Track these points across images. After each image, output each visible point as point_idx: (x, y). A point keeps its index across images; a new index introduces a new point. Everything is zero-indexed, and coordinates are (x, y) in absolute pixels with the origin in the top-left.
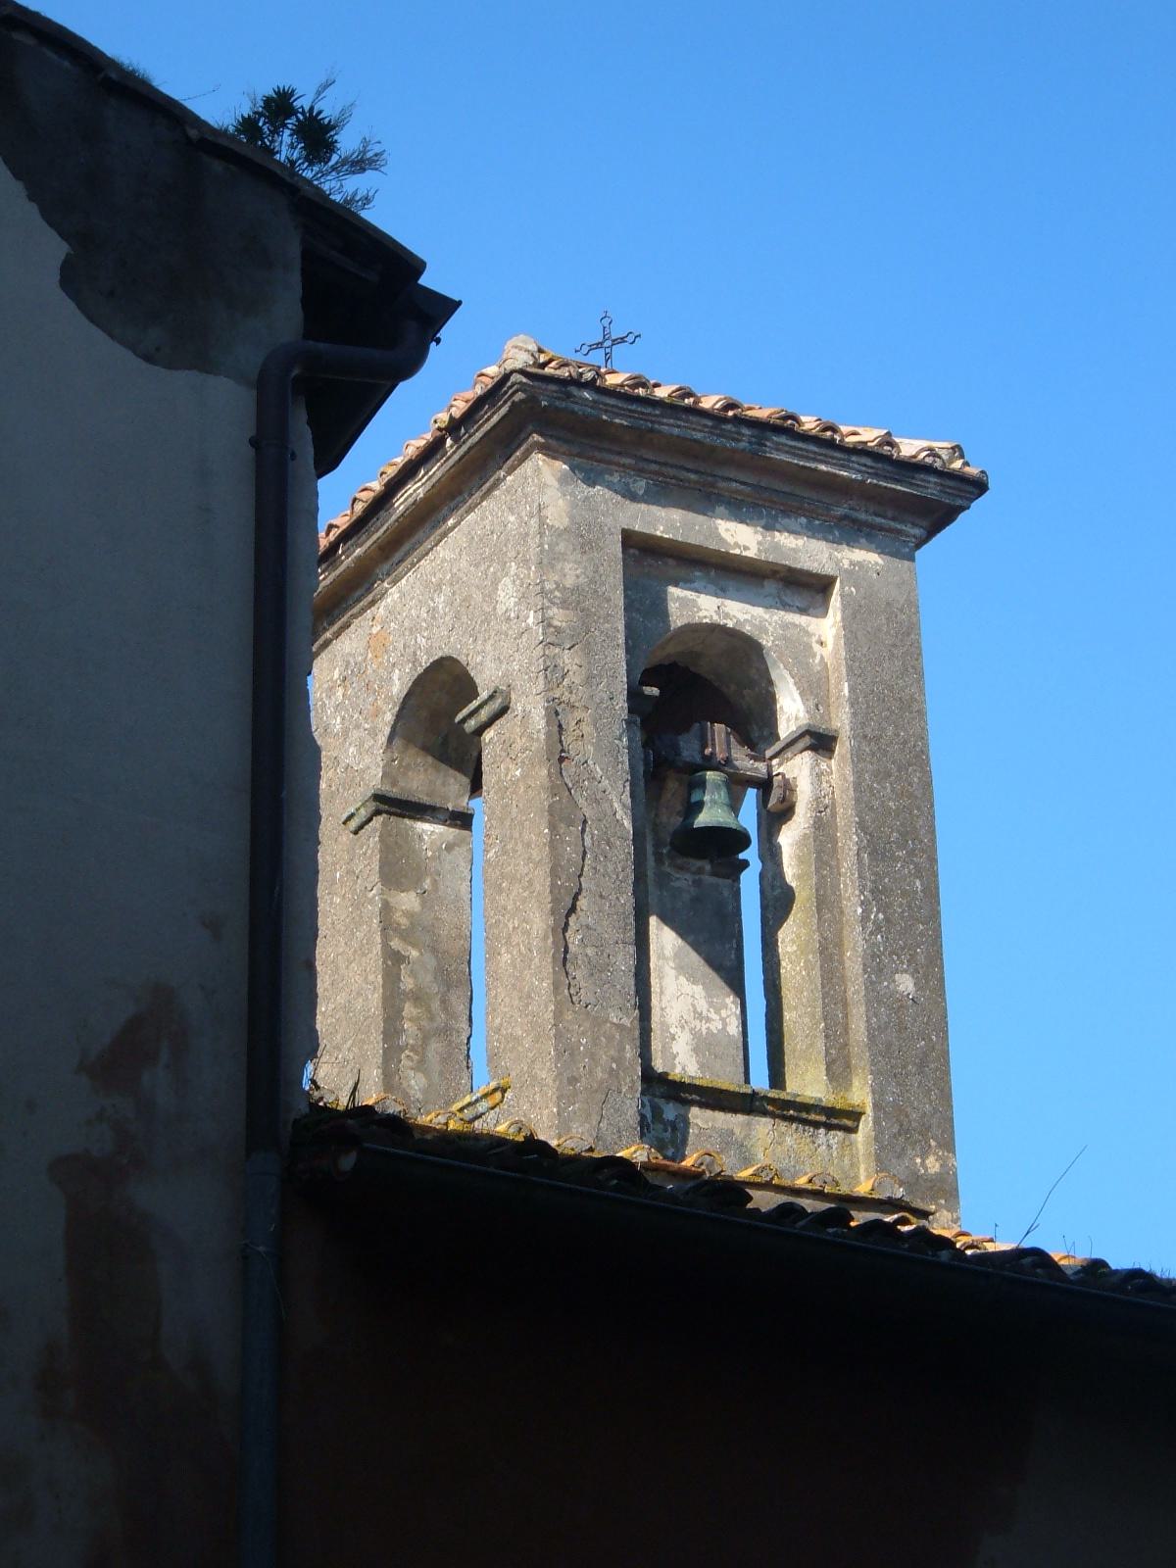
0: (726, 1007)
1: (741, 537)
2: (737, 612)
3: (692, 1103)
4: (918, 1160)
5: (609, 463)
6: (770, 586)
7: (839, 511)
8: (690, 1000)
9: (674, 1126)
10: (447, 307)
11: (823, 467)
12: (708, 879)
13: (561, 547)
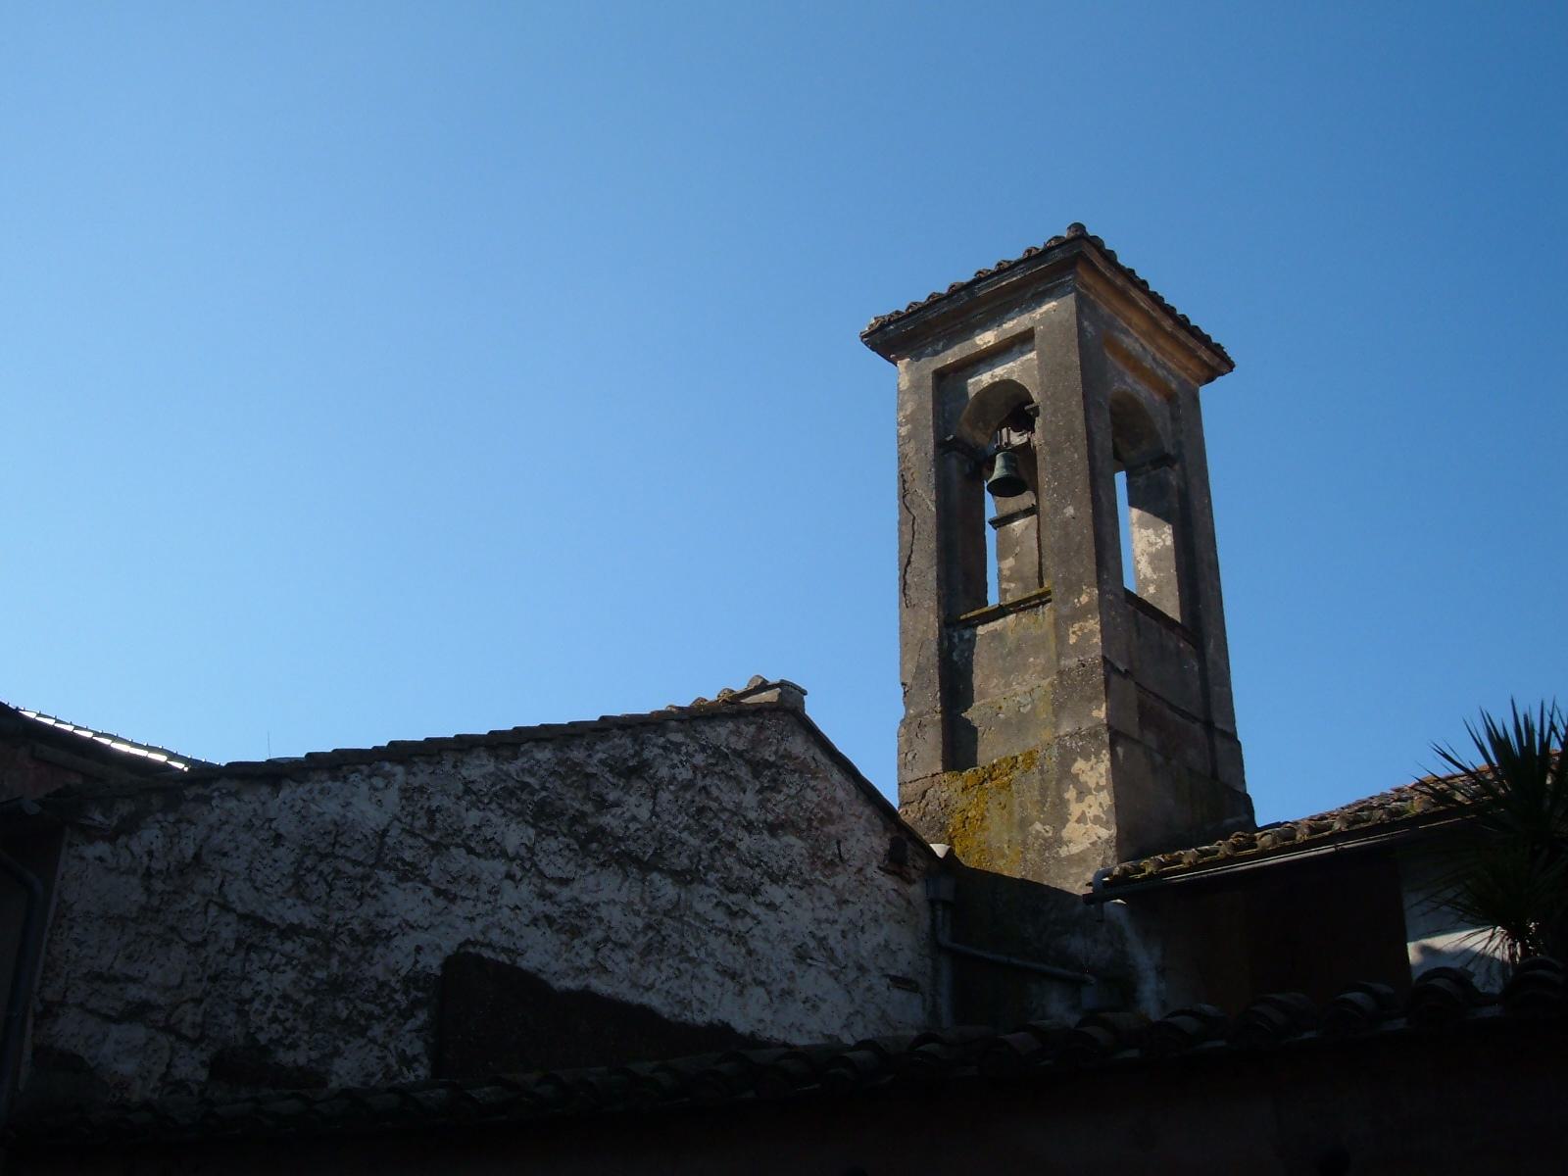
0: (1164, 533)
1: (987, 339)
2: (1000, 371)
3: (977, 625)
4: (1076, 600)
5: (925, 345)
6: (1016, 349)
7: (1029, 295)
8: (1146, 539)
9: (969, 640)
10: (1079, 228)
11: (1004, 283)
12: (1153, 473)
13: (906, 398)
